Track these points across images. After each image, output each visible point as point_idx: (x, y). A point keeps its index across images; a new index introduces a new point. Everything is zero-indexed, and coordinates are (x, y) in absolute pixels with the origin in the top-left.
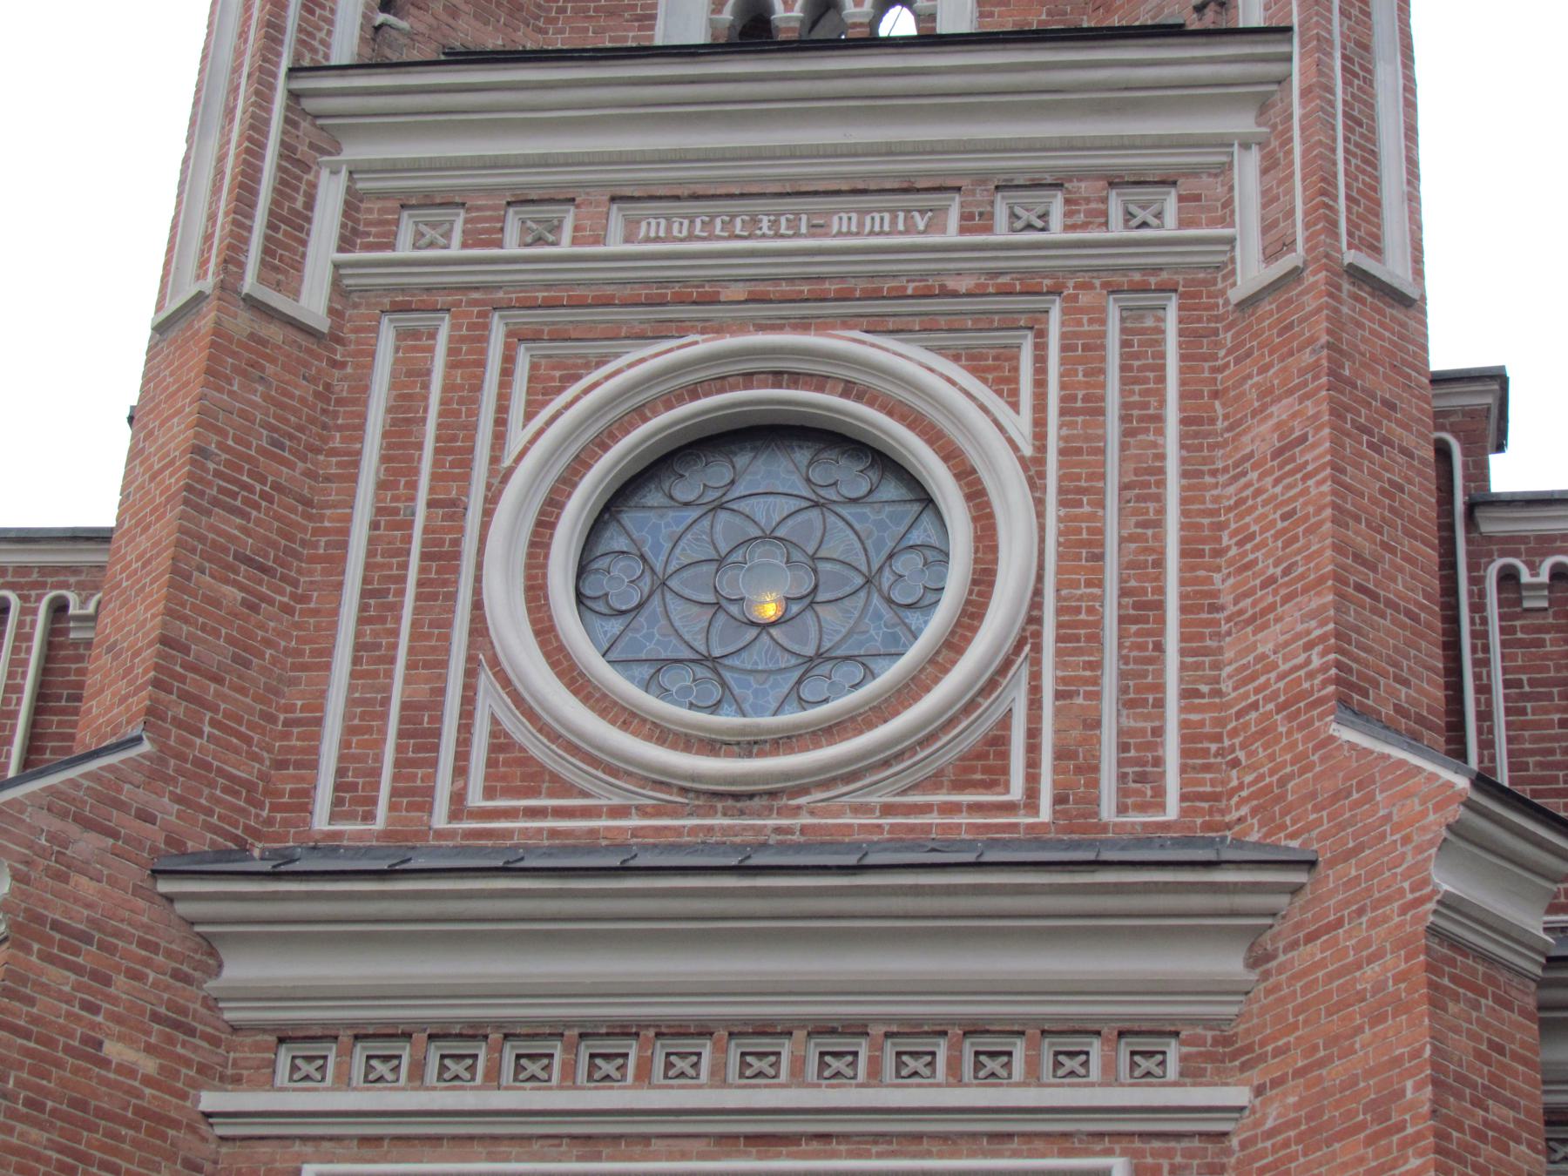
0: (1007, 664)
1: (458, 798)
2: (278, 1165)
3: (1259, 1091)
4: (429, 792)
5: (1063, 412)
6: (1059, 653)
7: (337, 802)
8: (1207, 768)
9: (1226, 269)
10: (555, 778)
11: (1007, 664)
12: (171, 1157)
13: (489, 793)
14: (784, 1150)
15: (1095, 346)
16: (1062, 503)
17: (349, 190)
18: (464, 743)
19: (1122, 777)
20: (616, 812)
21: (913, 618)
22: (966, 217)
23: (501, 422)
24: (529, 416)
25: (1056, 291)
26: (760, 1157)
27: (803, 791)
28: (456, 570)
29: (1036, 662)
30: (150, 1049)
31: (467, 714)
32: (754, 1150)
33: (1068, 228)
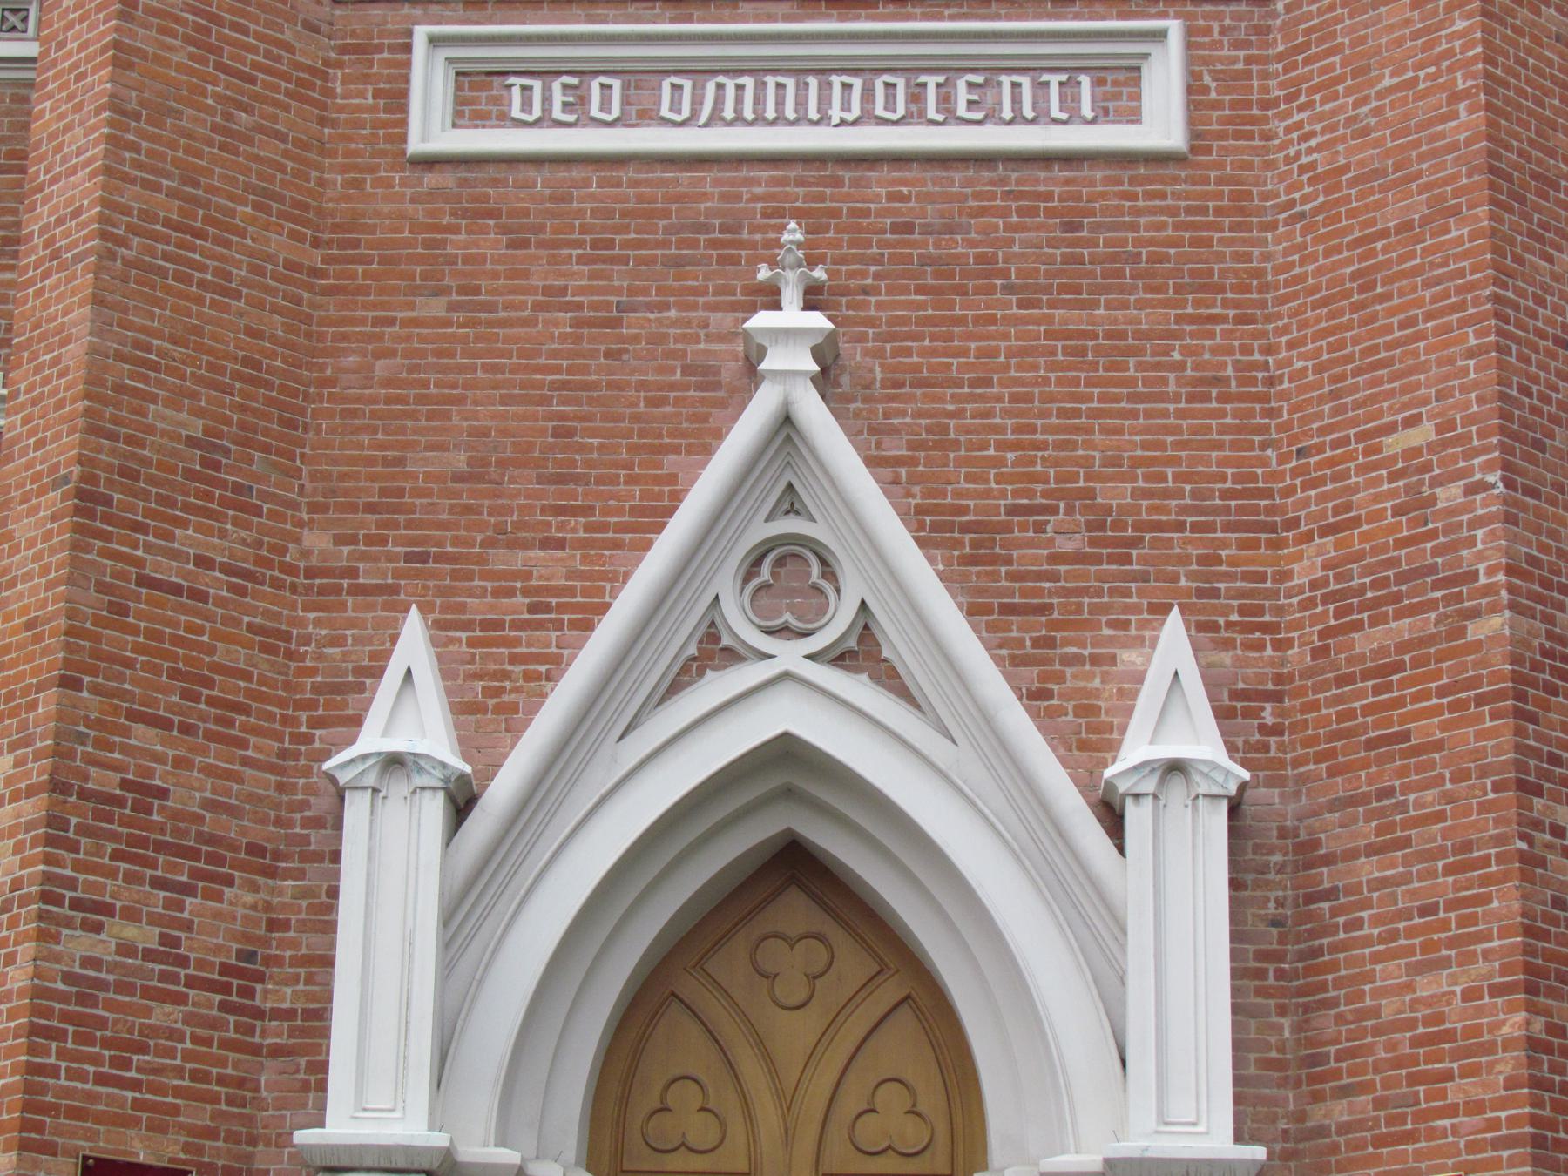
2: (389, 26)
12: (292, 20)
14: (863, 13)
26: (841, 19)
32: (835, 13)
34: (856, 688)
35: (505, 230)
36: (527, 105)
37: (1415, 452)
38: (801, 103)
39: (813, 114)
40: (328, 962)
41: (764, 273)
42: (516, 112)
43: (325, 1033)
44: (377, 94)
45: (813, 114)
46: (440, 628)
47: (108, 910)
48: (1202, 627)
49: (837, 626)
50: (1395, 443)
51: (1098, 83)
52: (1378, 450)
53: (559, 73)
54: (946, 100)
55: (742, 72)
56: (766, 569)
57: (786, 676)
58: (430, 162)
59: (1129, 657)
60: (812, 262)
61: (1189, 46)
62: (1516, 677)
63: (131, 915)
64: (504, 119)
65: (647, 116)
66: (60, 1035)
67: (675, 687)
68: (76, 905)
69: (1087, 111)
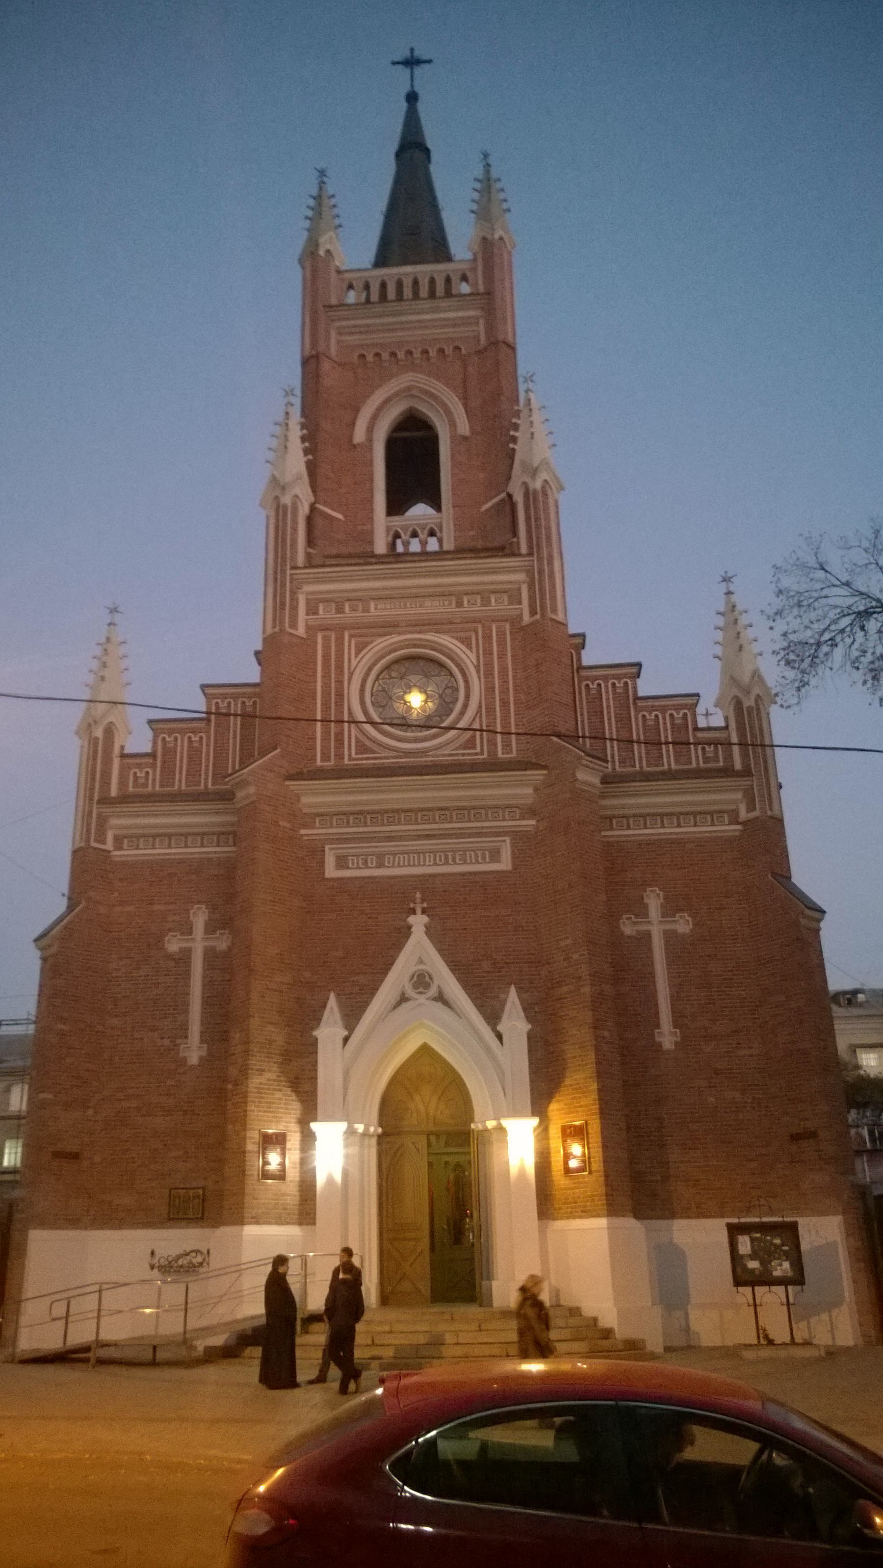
0: (474, 719)
1: (350, 755)
3: (538, 821)
4: (343, 755)
5: (484, 654)
6: (486, 716)
7: (322, 757)
8: (522, 743)
9: (520, 616)
10: (371, 749)
11: (474, 719)
13: (357, 754)
15: (491, 637)
16: (485, 678)
17: (307, 599)
18: (350, 742)
19: (503, 745)
20: (386, 758)
21: (451, 706)
22: (457, 602)
23: (349, 659)
24: (356, 657)
25: (480, 622)
27: (429, 752)
28: (343, 699)
29: (481, 717)
30: (290, 822)
31: (350, 735)
33: (482, 605)
34: (439, 1005)
35: (349, 895)
36: (353, 863)
37: (567, 946)
38: (419, 859)
39: (422, 863)
40: (316, 1078)
41: (412, 905)
42: (350, 866)
43: (316, 1096)
44: (317, 862)
45: (422, 863)
46: (338, 995)
47: (263, 1070)
48: (520, 988)
49: (433, 991)
50: (563, 944)
51: (491, 852)
52: (558, 944)
53: (360, 855)
54: (454, 860)
55: (405, 853)
56: (415, 976)
57: (420, 1004)
58: (332, 879)
59: (502, 996)
60: (423, 901)
61: (511, 843)
62: (592, 1001)
63: (270, 1071)
64: (348, 868)
65: (380, 865)
66: (254, 1102)
67: (395, 1008)
68: (257, 1070)
69: (487, 860)
